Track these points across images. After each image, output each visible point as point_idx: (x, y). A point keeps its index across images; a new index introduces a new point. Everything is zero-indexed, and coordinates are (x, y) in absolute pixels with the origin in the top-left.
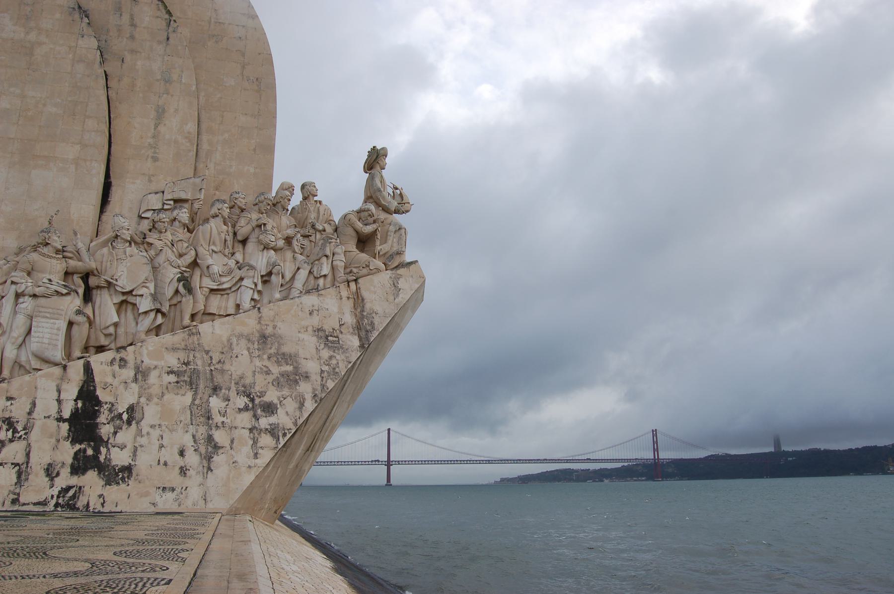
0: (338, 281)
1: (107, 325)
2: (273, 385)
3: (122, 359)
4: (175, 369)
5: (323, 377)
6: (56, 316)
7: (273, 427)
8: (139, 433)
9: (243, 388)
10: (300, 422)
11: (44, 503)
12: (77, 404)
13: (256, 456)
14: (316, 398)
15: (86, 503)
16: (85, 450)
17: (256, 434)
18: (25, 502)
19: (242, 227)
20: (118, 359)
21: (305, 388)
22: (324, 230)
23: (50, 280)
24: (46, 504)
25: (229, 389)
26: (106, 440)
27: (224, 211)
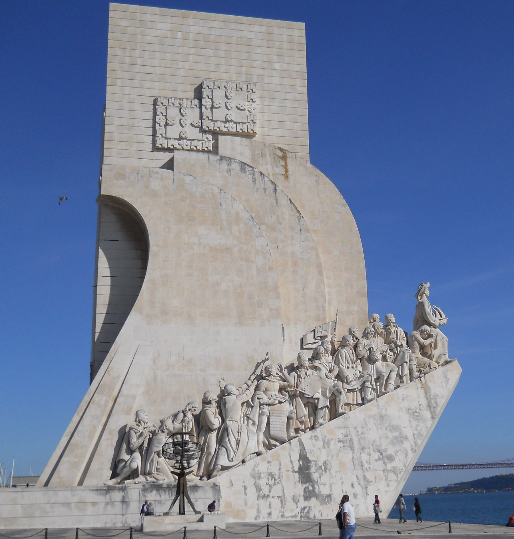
0: (414, 378)
1: (302, 416)
2: (391, 444)
3: (315, 436)
4: (342, 439)
5: (415, 438)
6: (281, 415)
7: (394, 468)
8: (331, 477)
9: (376, 447)
10: (407, 465)
11: (295, 516)
12: (300, 463)
13: (388, 485)
14: (413, 451)
15: (314, 515)
16: (308, 488)
17: (387, 474)
18: (288, 516)
19: (360, 350)
20: (314, 436)
21: (407, 445)
22: (402, 345)
23: (275, 395)
24: (296, 517)
25: (369, 449)
26: (317, 481)
27: (351, 342)
